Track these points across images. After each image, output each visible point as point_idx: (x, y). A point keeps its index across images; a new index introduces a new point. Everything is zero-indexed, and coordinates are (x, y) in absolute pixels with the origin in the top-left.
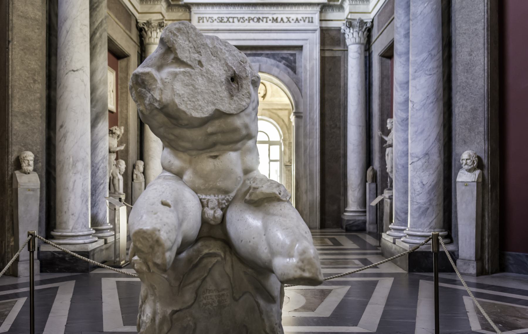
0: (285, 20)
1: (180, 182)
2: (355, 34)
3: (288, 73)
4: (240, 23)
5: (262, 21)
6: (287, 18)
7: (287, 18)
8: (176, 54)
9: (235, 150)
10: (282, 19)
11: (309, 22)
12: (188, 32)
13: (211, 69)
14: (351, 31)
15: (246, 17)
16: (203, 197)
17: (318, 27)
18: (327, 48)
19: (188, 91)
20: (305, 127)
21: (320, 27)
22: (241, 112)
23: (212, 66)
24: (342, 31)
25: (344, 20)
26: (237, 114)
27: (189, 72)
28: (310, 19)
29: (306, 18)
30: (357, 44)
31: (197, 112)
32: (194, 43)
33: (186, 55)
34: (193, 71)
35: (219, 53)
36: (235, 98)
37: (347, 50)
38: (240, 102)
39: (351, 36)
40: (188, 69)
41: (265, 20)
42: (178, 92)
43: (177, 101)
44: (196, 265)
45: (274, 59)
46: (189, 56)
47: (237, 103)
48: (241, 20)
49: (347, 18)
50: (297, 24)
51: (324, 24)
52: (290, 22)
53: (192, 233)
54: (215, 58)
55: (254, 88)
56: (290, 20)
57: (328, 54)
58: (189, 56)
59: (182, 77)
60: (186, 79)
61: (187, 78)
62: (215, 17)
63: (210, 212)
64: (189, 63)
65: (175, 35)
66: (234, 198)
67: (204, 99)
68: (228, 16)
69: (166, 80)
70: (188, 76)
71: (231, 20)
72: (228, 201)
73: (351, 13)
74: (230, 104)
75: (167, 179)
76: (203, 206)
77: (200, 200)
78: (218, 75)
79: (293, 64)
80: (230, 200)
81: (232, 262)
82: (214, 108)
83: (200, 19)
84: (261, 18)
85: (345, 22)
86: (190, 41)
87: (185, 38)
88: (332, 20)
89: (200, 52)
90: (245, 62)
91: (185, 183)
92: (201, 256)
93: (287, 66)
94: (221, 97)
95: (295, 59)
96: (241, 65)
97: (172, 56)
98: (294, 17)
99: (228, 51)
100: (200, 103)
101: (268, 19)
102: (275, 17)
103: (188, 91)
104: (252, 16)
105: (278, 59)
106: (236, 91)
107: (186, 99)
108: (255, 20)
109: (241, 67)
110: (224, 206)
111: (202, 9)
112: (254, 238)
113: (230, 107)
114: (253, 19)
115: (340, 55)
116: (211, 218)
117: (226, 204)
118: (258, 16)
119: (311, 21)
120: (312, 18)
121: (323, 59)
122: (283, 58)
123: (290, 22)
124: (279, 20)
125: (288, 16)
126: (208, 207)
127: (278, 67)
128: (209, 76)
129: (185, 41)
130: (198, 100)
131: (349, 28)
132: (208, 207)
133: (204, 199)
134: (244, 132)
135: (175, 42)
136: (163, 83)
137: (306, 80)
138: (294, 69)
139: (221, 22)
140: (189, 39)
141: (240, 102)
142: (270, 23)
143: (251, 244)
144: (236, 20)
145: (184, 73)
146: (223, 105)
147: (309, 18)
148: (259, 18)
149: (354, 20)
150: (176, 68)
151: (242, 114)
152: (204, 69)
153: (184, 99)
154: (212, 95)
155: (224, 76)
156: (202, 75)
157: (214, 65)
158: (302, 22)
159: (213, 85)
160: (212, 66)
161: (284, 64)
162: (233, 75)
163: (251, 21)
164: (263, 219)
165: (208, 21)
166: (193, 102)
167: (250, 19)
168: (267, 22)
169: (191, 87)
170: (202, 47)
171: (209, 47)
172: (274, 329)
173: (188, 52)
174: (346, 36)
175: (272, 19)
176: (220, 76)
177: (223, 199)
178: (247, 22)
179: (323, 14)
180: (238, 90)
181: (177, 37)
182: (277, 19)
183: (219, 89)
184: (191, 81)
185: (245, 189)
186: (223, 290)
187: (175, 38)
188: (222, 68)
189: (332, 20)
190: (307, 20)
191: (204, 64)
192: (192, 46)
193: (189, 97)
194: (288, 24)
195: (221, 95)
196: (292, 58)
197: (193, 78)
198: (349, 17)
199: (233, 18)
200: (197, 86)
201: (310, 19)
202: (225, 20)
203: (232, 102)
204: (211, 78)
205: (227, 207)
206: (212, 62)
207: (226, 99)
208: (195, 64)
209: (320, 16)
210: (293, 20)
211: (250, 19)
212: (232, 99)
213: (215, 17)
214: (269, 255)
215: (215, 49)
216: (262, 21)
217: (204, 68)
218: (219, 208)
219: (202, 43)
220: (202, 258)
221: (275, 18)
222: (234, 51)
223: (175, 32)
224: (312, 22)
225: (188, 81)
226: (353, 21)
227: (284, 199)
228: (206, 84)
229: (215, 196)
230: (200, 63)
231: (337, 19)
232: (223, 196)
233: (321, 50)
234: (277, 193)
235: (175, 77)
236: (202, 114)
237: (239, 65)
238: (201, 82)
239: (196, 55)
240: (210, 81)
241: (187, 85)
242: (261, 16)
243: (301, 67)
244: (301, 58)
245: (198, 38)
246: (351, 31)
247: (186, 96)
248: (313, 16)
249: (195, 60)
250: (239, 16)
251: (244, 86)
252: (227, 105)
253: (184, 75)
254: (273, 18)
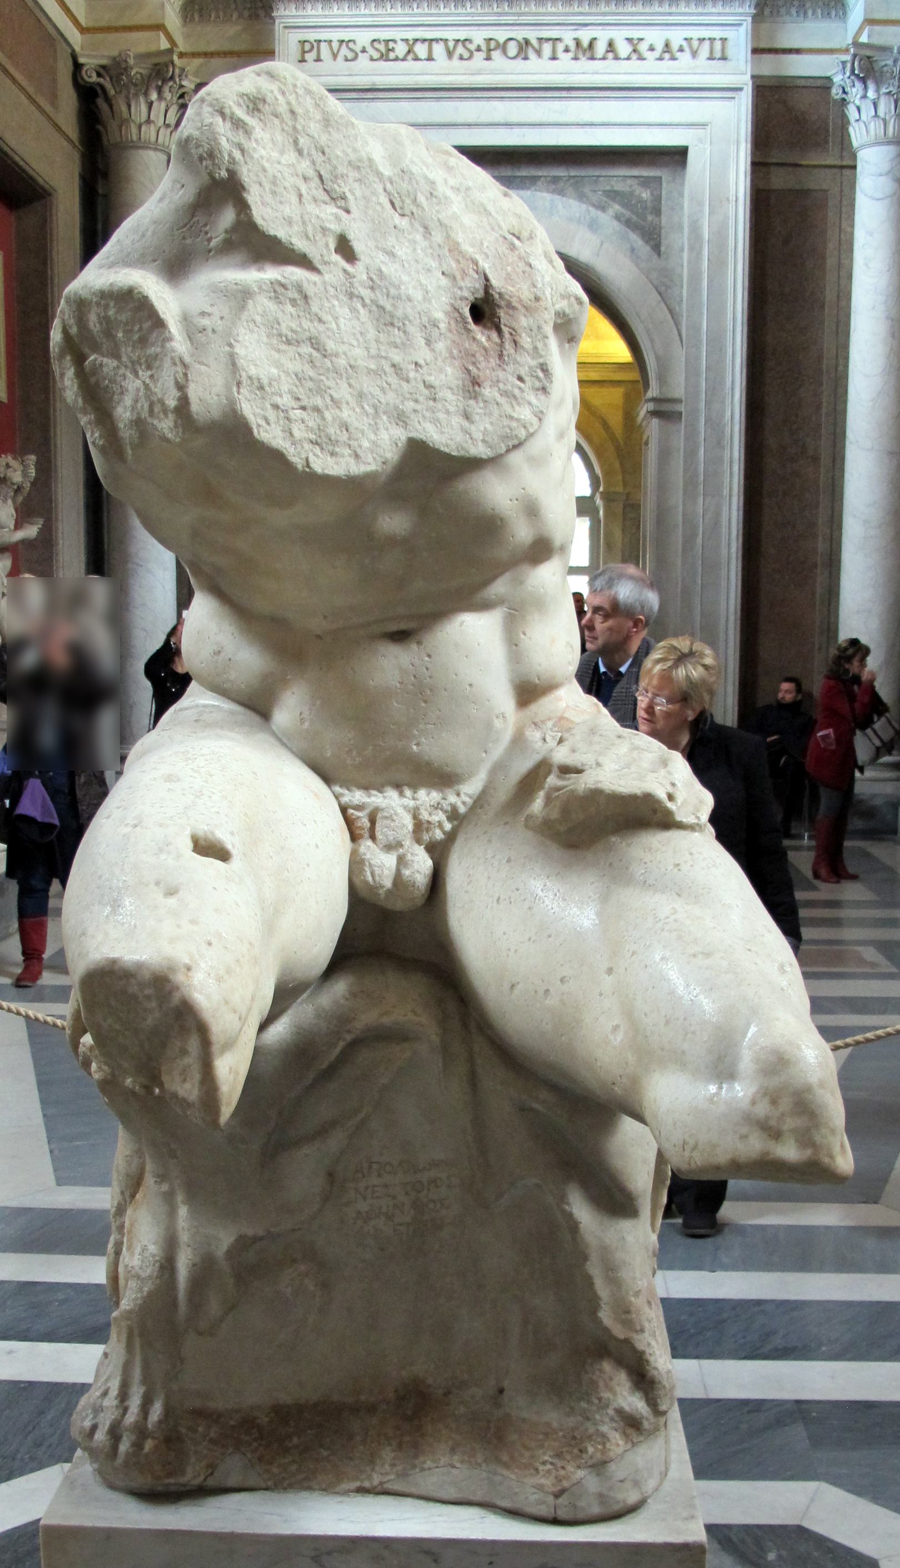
1: (263, 737)
2: (886, 106)
3: (633, 250)
4: (455, 62)
5: (539, 53)
6: (629, 40)
7: (629, 40)
8: (243, 206)
9: (485, 606)
10: (611, 46)
11: (711, 58)
12: (293, 112)
13: (390, 269)
14: (871, 94)
15: (479, 37)
16: (357, 796)
17: (749, 76)
18: (776, 156)
19: (295, 366)
20: (691, 454)
21: (753, 77)
22: (508, 451)
23: (391, 254)
24: (836, 93)
25: (847, 50)
26: (493, 462)
27: (300, 288)
28: (718, 45)
29: (701, 40)
30: (889, 143)
31: (332, 454)
32: (319, 158)
33: (287, 211)
34: (313, 277)
35: (422, 199)
36: (487, 392)
37: (854, 167)
38: (507, 408)
39: (868, 111)
40: (295, 273)
41: (547, 48)
42: (253, 371)
43: (250, 409)
44: (330, 1072)
45: (581, 197)
46: (296, 218)
47: (496, 412)
48: (460, 50)
49: (856, 44)
50: (667, 64)
51: (770, 67)
52: (641, 58)
53: (315, 950)
54: (404, 223)
55: (561, 346)
56: (643, 47)
57: (779, 180)
58: (296, 218)
59: (271, 306)
60: (288, 318)
61: (289, 308)
62: (363, 38)
63: (382, 865)
64: (300, 244)
65: (238, 124)
66: (480, 802)
67: (361, 396)
69: (205, 322)
70: (293, 302)
72: (453, 815)
73: (870, 22)
74: (467, 416)
75: (208, 725)
76: (354, 838)
77: (344, 810)
78: (418, 295)
79: (650, 218)
80: (462, 810)
81: (471, 1060)
82: (401, 435)
84: (534, 42)
85: (848, 58)
86: (300, 152)
87: (279, 138)
88: (798, 51)
89: (344, 198)
90: (525, 234)
91: (283, 741)
92: (349, 1038)
93: (628, 223)
94: (429, 386)
95: (658, 199)
96: (513, 247)
97: (228, 217)
99: (457, 190)
100: (345, 414)
101: (560, 47)
102: (585, 36)
103: (295, 366)
105: (594, 198)
106: (494, 361)
107: (285, 401)
108: (512, 49)
109: (512, 258)
110: (439, 835)
112: (562, 980)
113: (466, 432)
114: (503, 48)
115: (824, 187)
116: (388, 883)
117: (448, 826)
118: (520, 34)
119: (718, 55)
120: (724, 40)
121: (762, 201)
122: (613, 195)
123: (641, 58)
124: (601, 48)
125: (635, 33)
126: (373, 837)
127: (593, 226)
128: (383, 301)
129: (282, 152)
130: (336, 403)
131: (864, 81)
132: (373, 837)
133: (359, 808)
134: (522, 533)
135: (237, 155)
136: (193, 331)
137: (695, 277)
138: (653, 239)
139: (384, 57)
140: (296, 142)
141: (507, 408)
142: (565, 58)
143: (551, 1002)
144: (438, 49)
145: (277, 290)
146: (436, 421)
147: (712, 40)
148: (527, 42)
149: (884, 49)
150: (244, 265)
151: (516, 458)
152: (359, 270)
153: (279, 401)
154: (393, 380)
155: (445, 299)
156: (351, 296)
157: (401, 252)
158: (685, 58)
159: (397, 336)
160: (391, 254)
161: (617, 217)
162: (480, 294)
163: (496, 55)
164: (604, 899)
166: (317, 409)
167: (491, 47)
168: (554, 58)
169: (306, 349)
170: (353, 174)
171: (379, 175)
172: (628, 1312)
173: (294, 199)
174: (852, 113)
175: (572, 45)
176: (426, 299)
177: (437, 807)
179: (765, 26)
180: (501, 356)
181: (248, 132)
183: (423, 354)
184: (306, 324)
185: (523, 766)
186: (435, 1164)
187: (241, 138)
188: (434, 264)
189: (798, 51)
190: (705, 51)
191: (358, 246)
192: (311, 173)
193: (301, 393)
194: (634, 64)
195: (431, 379)
196: (645, 195)
197: (315, 308)
198: (864, 39)
200: (331, 345)
201: (718, 45)
203: (476, 408)
204: (388, 307)
205: (451, 837)
206: (391, 241)
207: (449, 395)
208: (321, 249)
209: (756, 33)
210: (652, 49)
211: (491, 47)
212: (475, 396)
214: (631, 1058)
215: (405, 186)
216: (539, 53)
217: (360, 266)
218: (418, 841)
219: (353, 156)
220: (356, 1044)
221: (585, 44)
222: (483, 188)
223: (240, 113)
224: (724, 58)
225: (294, 325)
226: (877, 56)
227: (691, 820)
228: (372, 333)
229: (402, 794)
230: (345, 248)
231: (819, 49)
232: (435, 796)
233: (754, 164)
234: (661, 794)
235: (243, 308)
236: (352, 461)
237: (503, 249)
238: (347, 328)
239: (329, 211)
240: (387, 320)
241: (288, 342)
242: (533, 35)
243: (680, 227)
244: (681, 195)
245: (336, 136)
246: (871, 94)
247: (285, 388)
248: (728, 33)
249: (324, 230)
250: (451, 34)
251: (525, 341)
252: (457, 421)
253: (277, 298)
254: (578, 43)
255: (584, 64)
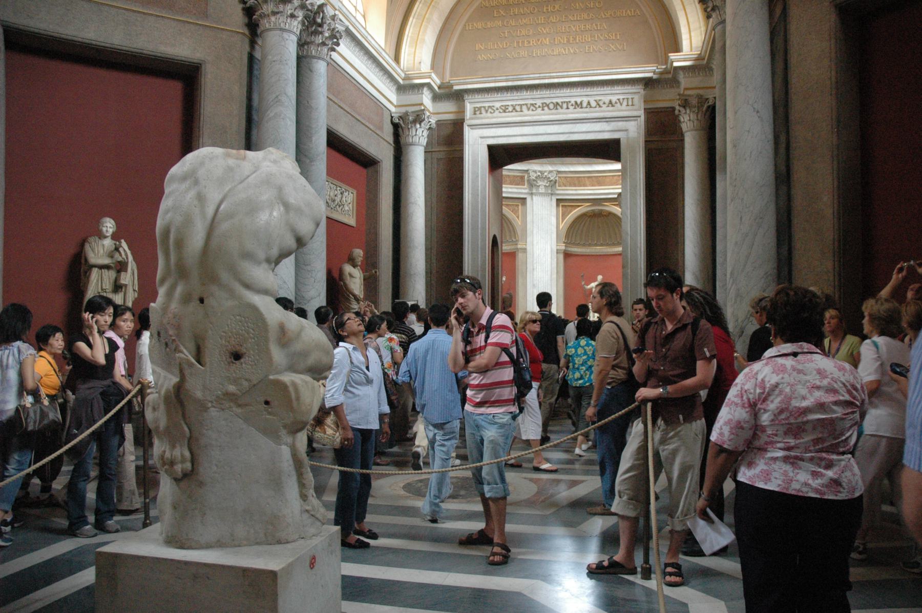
0: (593, 104)
2: (693, 116)
5: (562, 107)
10: (589, 103)
14: (688, 111)
41: (565, 106)
50: (611, 108)
56: (601, 103)
68: (514, 103)
71: (518, 108)
83: (476, 111)
98: (606, 99)
102: (579, 100)
104: (548, 101)
108: (551, 106)
111: (478, 97)
118: (555, 101)
124: (585, 105)
125: (598, 98)
139: (504, 111)
144: (524, 108)
148: (557, 103)
165: (487, 111)
178: (539, 110)
182: (581, 103)
190: (625, 103)
194: (597, 109)
199: (521, 105)
202: (510, 109)
213: (498, 105)
216: (562, 107)
233: (646, 141)
242: (559, 101)
246: (688, 111)
255: (579, 110)
